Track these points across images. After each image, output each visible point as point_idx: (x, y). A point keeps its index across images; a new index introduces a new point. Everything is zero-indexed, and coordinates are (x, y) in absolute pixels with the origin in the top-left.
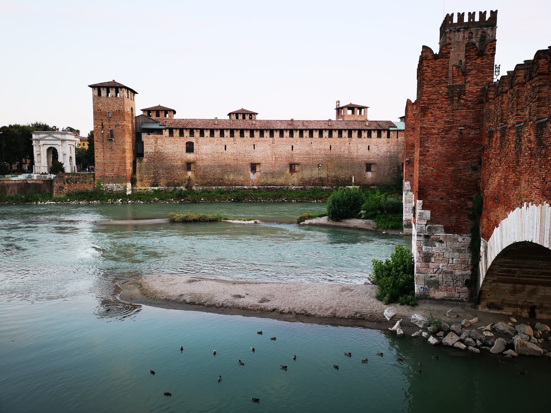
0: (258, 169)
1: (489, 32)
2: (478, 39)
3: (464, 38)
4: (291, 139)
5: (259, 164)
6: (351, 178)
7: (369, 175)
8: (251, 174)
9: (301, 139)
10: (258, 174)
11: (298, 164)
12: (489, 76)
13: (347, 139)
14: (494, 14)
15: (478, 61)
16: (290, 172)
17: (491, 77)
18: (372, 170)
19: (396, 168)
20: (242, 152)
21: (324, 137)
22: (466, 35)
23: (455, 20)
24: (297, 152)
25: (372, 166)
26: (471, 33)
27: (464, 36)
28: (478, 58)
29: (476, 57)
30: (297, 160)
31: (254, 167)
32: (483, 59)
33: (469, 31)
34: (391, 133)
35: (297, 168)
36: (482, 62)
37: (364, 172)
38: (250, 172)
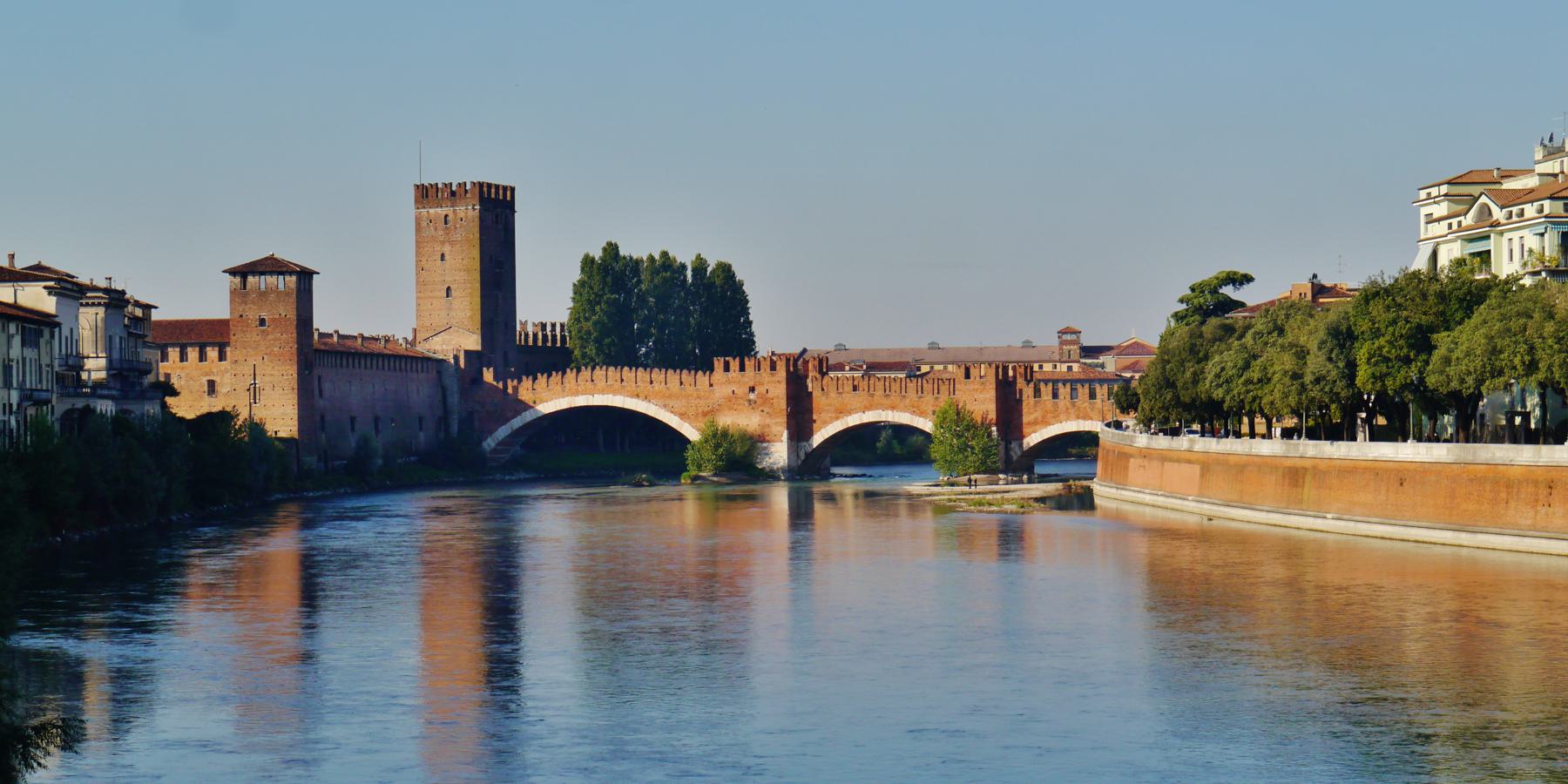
7: (422, 435)
14: (513, 190)
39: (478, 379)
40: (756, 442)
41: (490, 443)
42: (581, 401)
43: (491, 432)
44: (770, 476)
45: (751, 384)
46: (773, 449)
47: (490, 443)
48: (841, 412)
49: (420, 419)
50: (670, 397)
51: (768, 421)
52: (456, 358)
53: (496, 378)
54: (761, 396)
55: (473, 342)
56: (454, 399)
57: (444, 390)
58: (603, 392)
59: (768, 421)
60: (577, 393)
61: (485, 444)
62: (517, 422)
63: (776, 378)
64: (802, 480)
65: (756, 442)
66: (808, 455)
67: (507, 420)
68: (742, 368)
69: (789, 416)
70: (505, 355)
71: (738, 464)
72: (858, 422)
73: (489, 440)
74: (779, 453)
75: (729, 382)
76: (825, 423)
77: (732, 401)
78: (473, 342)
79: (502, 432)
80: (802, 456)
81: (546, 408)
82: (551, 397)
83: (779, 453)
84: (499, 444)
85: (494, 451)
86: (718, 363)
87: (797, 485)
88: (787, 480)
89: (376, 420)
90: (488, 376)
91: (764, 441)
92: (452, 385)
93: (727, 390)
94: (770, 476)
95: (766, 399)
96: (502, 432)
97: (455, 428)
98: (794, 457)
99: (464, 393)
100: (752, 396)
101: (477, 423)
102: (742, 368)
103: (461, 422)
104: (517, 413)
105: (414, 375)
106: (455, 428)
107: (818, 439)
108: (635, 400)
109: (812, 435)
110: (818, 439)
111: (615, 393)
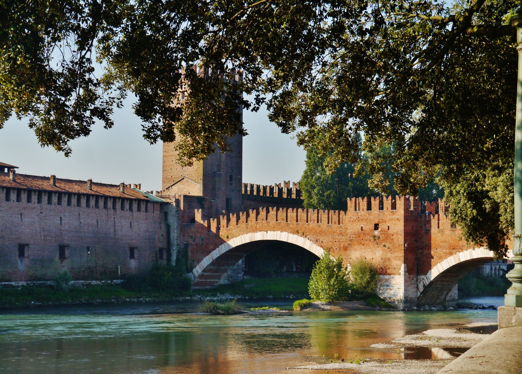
0: (26, 254)
4: (59, 207)
5: (28, 245)
6: (117, 268)
7: (133, 264)
8: (19, 261)
9: (69, 207)
10: (26, 261)
11: (68, 246)
13: (112, 211)
16: (60, 259)
18: (136, 256)
19: (154, 255)
20: (8, 225)
21: (91, 207)
24: (66, 227)
25: (136, 250)
30: (66, 240)
31: (22, 248)
34: (149, 204)
35: (67, 252)
37: (128, 259)
38: (17, 258)
39: (193, 220)
40: (375, 274)
41: (198, 270)
42: (259, 236)
43: (199, 261)
44: (389, 306)
45: (376, 221)
46: (393, 282)
47: (198, 270)
48: (454, 249)
49: (132, 250)
50: (321, 233)
51: (389, 255)
52: (177, 201)
53: (204, 217)
54: (383, 232)
55: (196, 190)
56: (174, 234)
57: (168, 227)
58: (273, 229)
59: (389, 255)
60: (255, 230)
61: (194, 271)
62: (216, 254)
63: (396, 216)
64: (418, 310)
65: (375, 274)
66: (425, 287)
67: (210, 252)
68: (369, 208)
69: (406, 251)
70: (228, 201)
71: (363, 296)
72: (468, 258)
73: (197, 267)
74: (397, 287)
75: (359, 220)
76: (441, 258)
77: (360, 238)
78: (196, 190)
79: (206, 261)
80: (421, 289)
81: (234, 242)
82: (238, 235)
83: (397, 287)
84: (204, 271)
85: (201, 276)
86: (350, 203)
87: (410, 316)
88: (404, 310)
89: (62, 249)
90: (198, 216)
91: (386, 273)
92: (173, 221)
93: (357, 227)
94: (389, 306)
95: (387, 236)
96: (206, 261)
97: (174, 257)
98: (412, 289)
99: (182, 229)
100: (376, 233)
101: (190, 254)
102: (369, 208)
103: (179, 252)
104: (216, 246)
105: (128, 213)
106: (174, 257)
107: (435, 272)
108: (295, 236)
109: (429, 267)
110: (435, 272)
111: (282, 230)
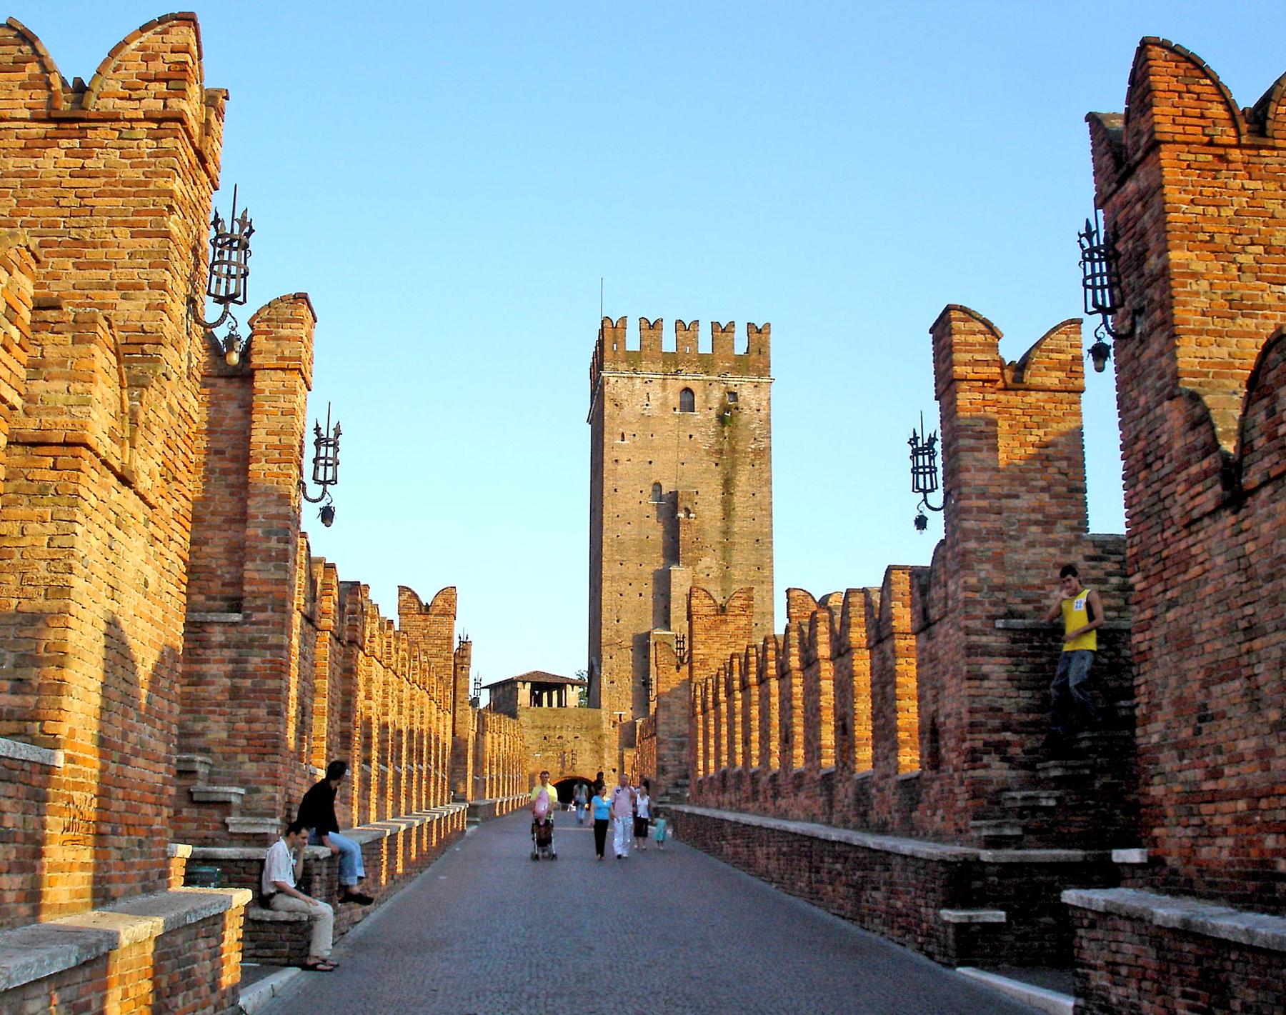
1: (746, 392)
2: (713, 414)
3: (664, 404)
12: (127, 290)
14: (758, 333)
15: (54, 162)
17: (144, 297)
22: (675, 399)
23: (633, 342)
26: (687, 390)
27: (666, 398)
28: (49, 141)
29: (38, 129)
32: (86, 152)
33: (681, 385)
36: (83, 173)
